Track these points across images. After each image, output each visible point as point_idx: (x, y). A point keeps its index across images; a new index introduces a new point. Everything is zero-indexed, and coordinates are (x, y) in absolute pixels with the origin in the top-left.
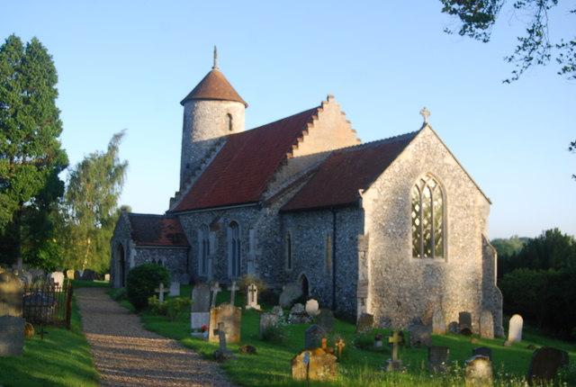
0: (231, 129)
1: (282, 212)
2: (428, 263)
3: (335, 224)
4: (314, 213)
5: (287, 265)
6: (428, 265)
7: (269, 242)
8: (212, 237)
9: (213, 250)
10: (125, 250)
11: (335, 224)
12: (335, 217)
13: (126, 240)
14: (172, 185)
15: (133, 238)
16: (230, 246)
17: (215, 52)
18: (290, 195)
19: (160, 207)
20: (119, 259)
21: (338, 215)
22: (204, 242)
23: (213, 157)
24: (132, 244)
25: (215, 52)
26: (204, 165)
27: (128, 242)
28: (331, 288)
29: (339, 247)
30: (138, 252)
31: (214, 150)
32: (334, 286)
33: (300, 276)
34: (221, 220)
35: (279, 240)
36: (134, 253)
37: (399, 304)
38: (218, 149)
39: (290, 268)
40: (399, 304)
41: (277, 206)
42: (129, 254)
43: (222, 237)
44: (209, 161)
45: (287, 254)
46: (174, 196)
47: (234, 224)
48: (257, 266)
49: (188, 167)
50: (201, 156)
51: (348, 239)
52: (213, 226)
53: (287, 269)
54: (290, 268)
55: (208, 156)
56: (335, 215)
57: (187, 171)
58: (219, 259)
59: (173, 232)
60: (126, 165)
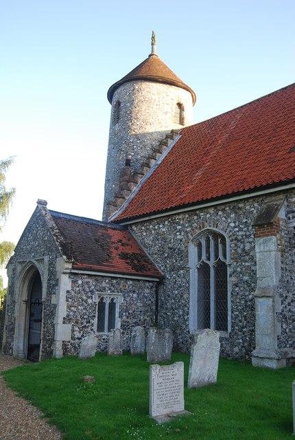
0: (181, 122)
10: (45, 279)
13: (46, 259)
17: (153, 38)
20: (25, 297)
23: (165, 153)
24: (63, 265)
25: (153, 38)
26: (153, 162)
27: (52, 264)
30: (74, 282)
31: (172, 138)
36: (65, 283)
38: (171, 143)
42: (54, 285)
44: (161, 158)
50: (145, 153)
55: (157, 151)
60: (14, 191)
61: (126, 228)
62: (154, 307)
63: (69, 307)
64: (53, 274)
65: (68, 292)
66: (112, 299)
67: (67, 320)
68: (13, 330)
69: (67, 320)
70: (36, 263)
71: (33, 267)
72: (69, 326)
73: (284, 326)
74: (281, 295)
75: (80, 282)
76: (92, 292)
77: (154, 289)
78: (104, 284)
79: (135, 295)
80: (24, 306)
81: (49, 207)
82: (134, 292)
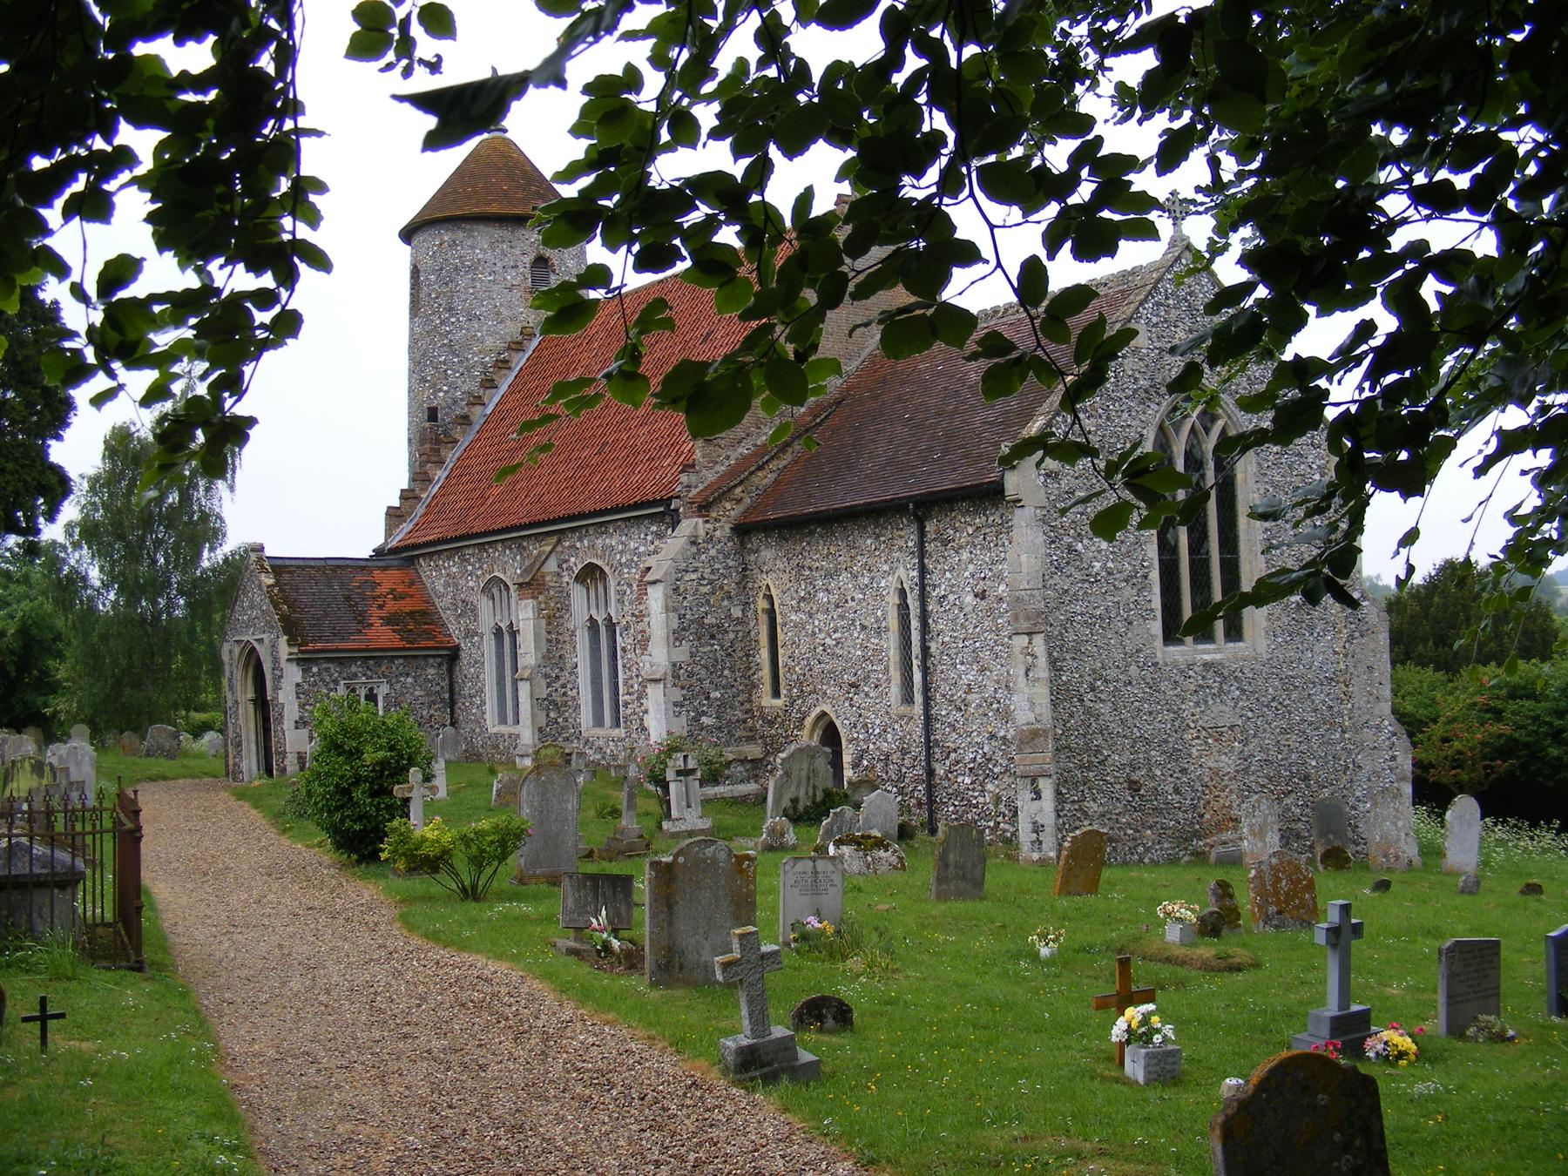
1: (743, 531)
2: (1207, 657)
3: (922, 554)
4: (850, 525)
5: (767, 687)
6: (1207, 666)
7: (709, 620)
8: (525, 615)
9: (529, 654)
10: (267, 667)
11: (922, 554)
12: (922, 533)
14: (390, 473)
15: (286, 631)
16: (582, 640)
18: (765, 478)
19: (360, 536)
20: (251, 695)
21: (930, 527)
22: (498, 633)
26: (478, 410)
27: (274, 646)
28: (917, 750)
29: (939, 624)
32: (929, 745)
33: (809, 721)
34: (552, 566)
35: (737, 612)
37: (1134, 786)
38: (519, 361)
39: (776, 693)
40: (1134, 786)
41: (731, 511)
43: (553, 618)
45: (764, 654)
46: (397, 504)
47: (591, 575)
48: (677, 695)
49: (432, 414)
50: (472, 385)
51: (969, 599)
52: (532, 585)
53: (767, 701)
54: (776, 693)
55: (489, 384)
56: (922, 533)
57: (432, 432)
58: (552, 681)
59: (406, 606)
61: (411, 560)
62: (447, 696)
63: (302, 706)
64: (276, 660)
65: (298, 685)
66: (371, 689)
67: (300, 723)
68: (239, 744)
69: (300, 723)
70: (256, 645)
71: (253, 649)
72: (305, 732)
73: (552, 715)
74: (546, 676)
75: (315, 669)
76: (336, 682)
77: (445, 667)
78: (354, 669)
79: (410, 680)
80: (251, 707)
81: (268, 552)
82: (408, 675)
